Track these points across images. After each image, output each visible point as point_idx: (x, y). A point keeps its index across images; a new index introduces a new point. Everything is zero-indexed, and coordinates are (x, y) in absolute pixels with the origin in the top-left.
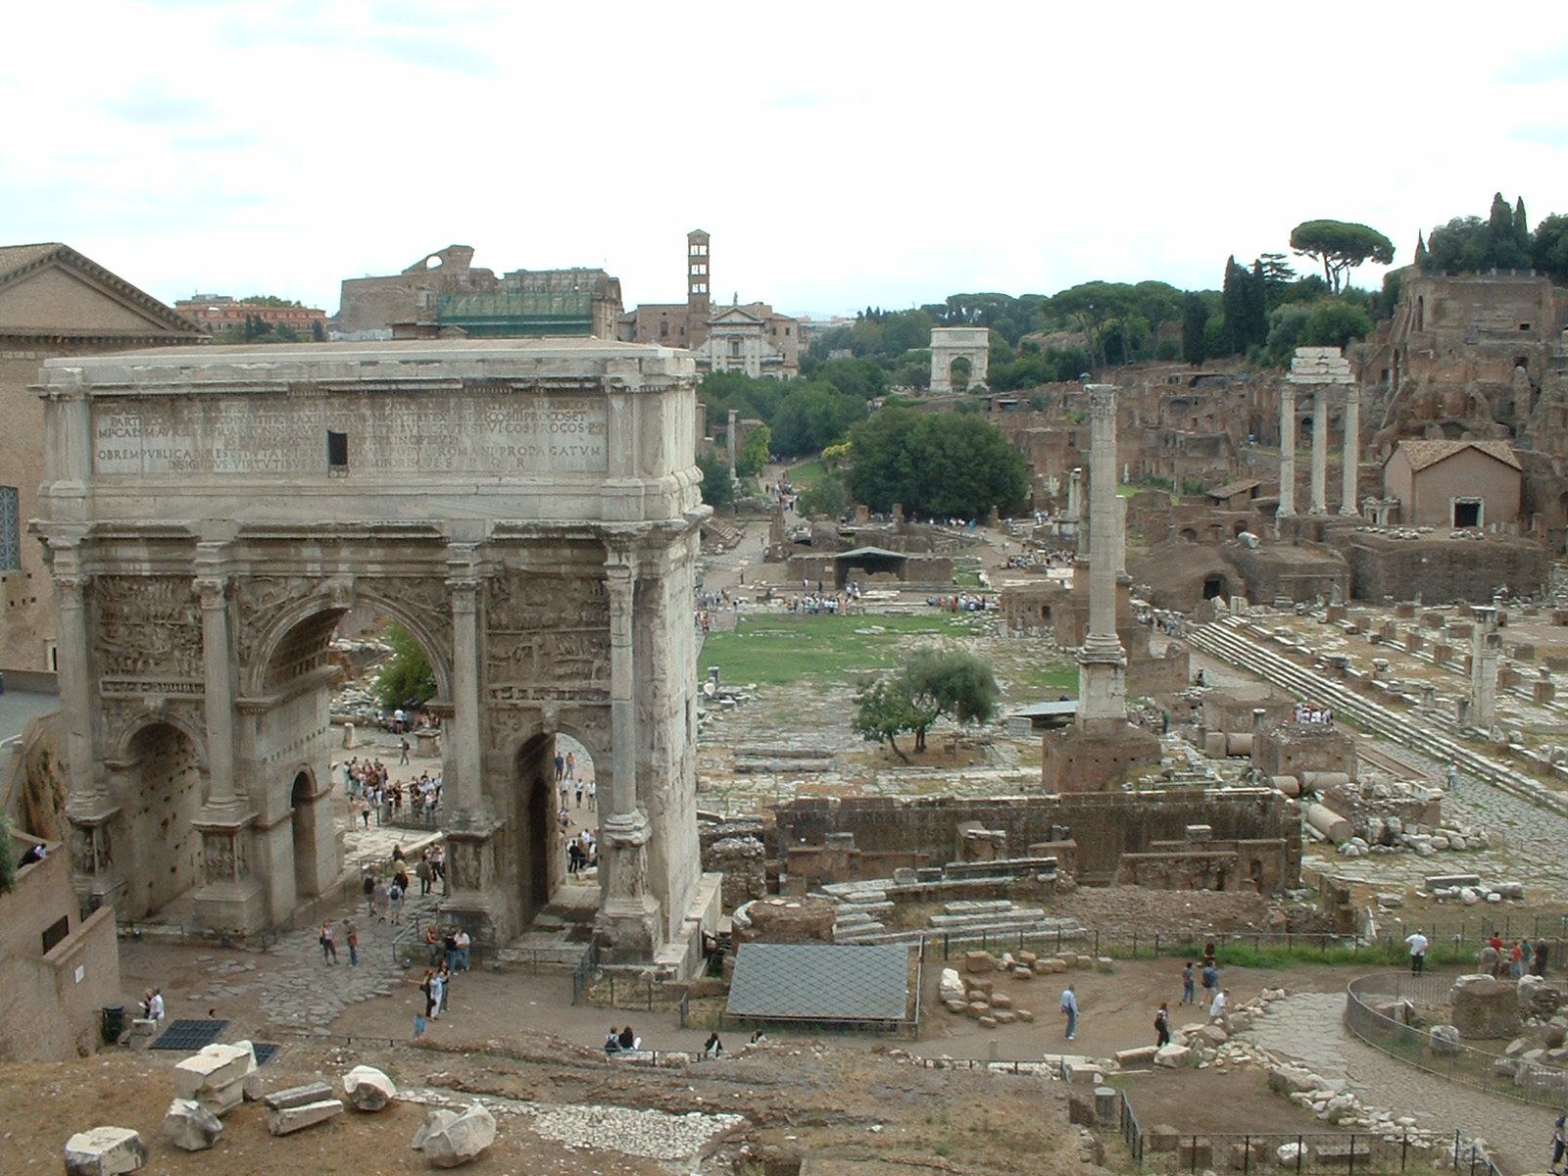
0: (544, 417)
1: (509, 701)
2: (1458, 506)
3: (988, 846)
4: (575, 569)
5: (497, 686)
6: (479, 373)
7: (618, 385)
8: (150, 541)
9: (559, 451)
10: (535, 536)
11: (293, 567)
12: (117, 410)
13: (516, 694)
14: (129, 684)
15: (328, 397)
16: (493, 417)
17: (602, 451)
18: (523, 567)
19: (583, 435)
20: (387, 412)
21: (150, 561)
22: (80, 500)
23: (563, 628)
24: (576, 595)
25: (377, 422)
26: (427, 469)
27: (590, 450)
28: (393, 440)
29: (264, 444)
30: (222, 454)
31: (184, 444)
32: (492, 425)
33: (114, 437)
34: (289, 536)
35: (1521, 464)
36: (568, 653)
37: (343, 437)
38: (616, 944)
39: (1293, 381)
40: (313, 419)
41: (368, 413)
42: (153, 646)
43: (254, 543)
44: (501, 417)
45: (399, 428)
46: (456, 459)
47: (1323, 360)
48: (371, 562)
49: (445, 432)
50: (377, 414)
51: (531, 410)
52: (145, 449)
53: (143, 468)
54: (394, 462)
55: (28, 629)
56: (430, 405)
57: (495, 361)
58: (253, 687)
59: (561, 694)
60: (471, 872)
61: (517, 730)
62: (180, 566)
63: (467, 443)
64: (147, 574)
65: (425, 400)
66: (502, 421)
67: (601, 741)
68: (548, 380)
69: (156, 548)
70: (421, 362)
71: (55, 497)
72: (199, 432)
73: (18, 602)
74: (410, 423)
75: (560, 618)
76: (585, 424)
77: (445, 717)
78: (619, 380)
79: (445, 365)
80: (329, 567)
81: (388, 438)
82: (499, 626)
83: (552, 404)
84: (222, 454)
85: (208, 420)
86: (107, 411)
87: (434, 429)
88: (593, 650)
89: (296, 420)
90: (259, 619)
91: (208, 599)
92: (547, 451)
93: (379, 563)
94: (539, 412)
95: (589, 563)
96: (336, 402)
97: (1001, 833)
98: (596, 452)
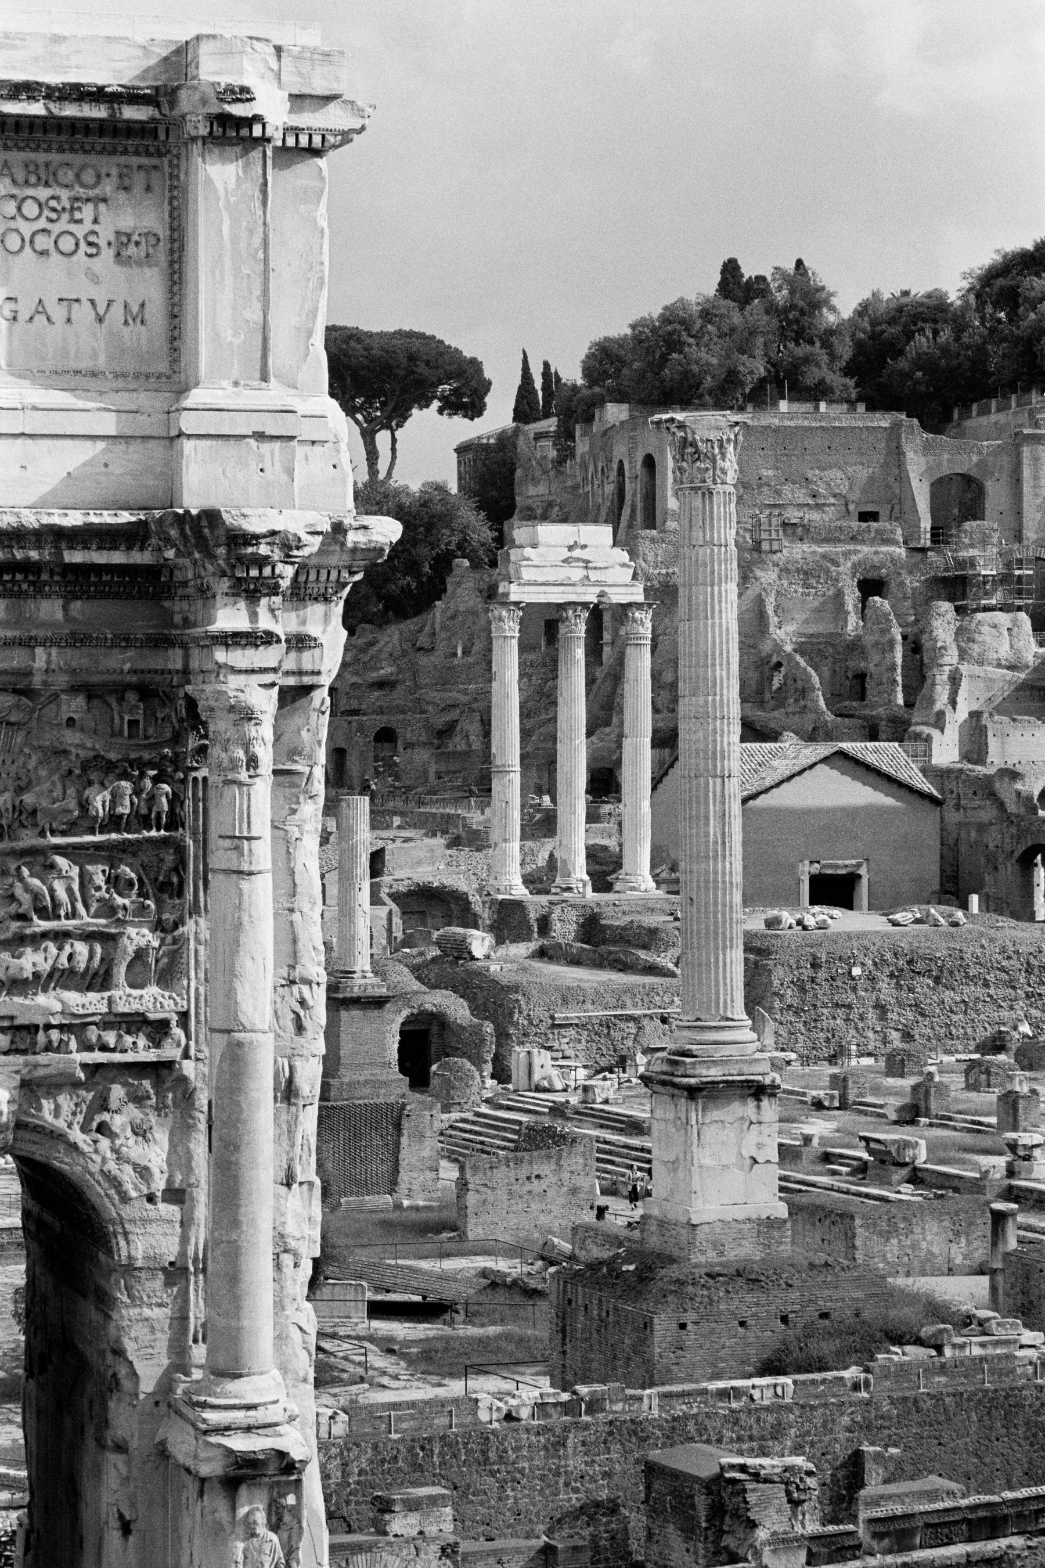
2: (816, 881)
3: (778, 1492)
4: (78, 658)
7: (238, 110)
17: (156, 312)
19: (96, 264)
23: (28, 839)
24: (71, 738)
27: (117, 311)
35: (941, 791)
36: (43, 913)
39: (513, 598)
47: (577, 553)
75: (18, 809)
76: (105, 234)
78: (243, 95)
95: (123, 641)
97: (799, 1461)
98: (136, 316)
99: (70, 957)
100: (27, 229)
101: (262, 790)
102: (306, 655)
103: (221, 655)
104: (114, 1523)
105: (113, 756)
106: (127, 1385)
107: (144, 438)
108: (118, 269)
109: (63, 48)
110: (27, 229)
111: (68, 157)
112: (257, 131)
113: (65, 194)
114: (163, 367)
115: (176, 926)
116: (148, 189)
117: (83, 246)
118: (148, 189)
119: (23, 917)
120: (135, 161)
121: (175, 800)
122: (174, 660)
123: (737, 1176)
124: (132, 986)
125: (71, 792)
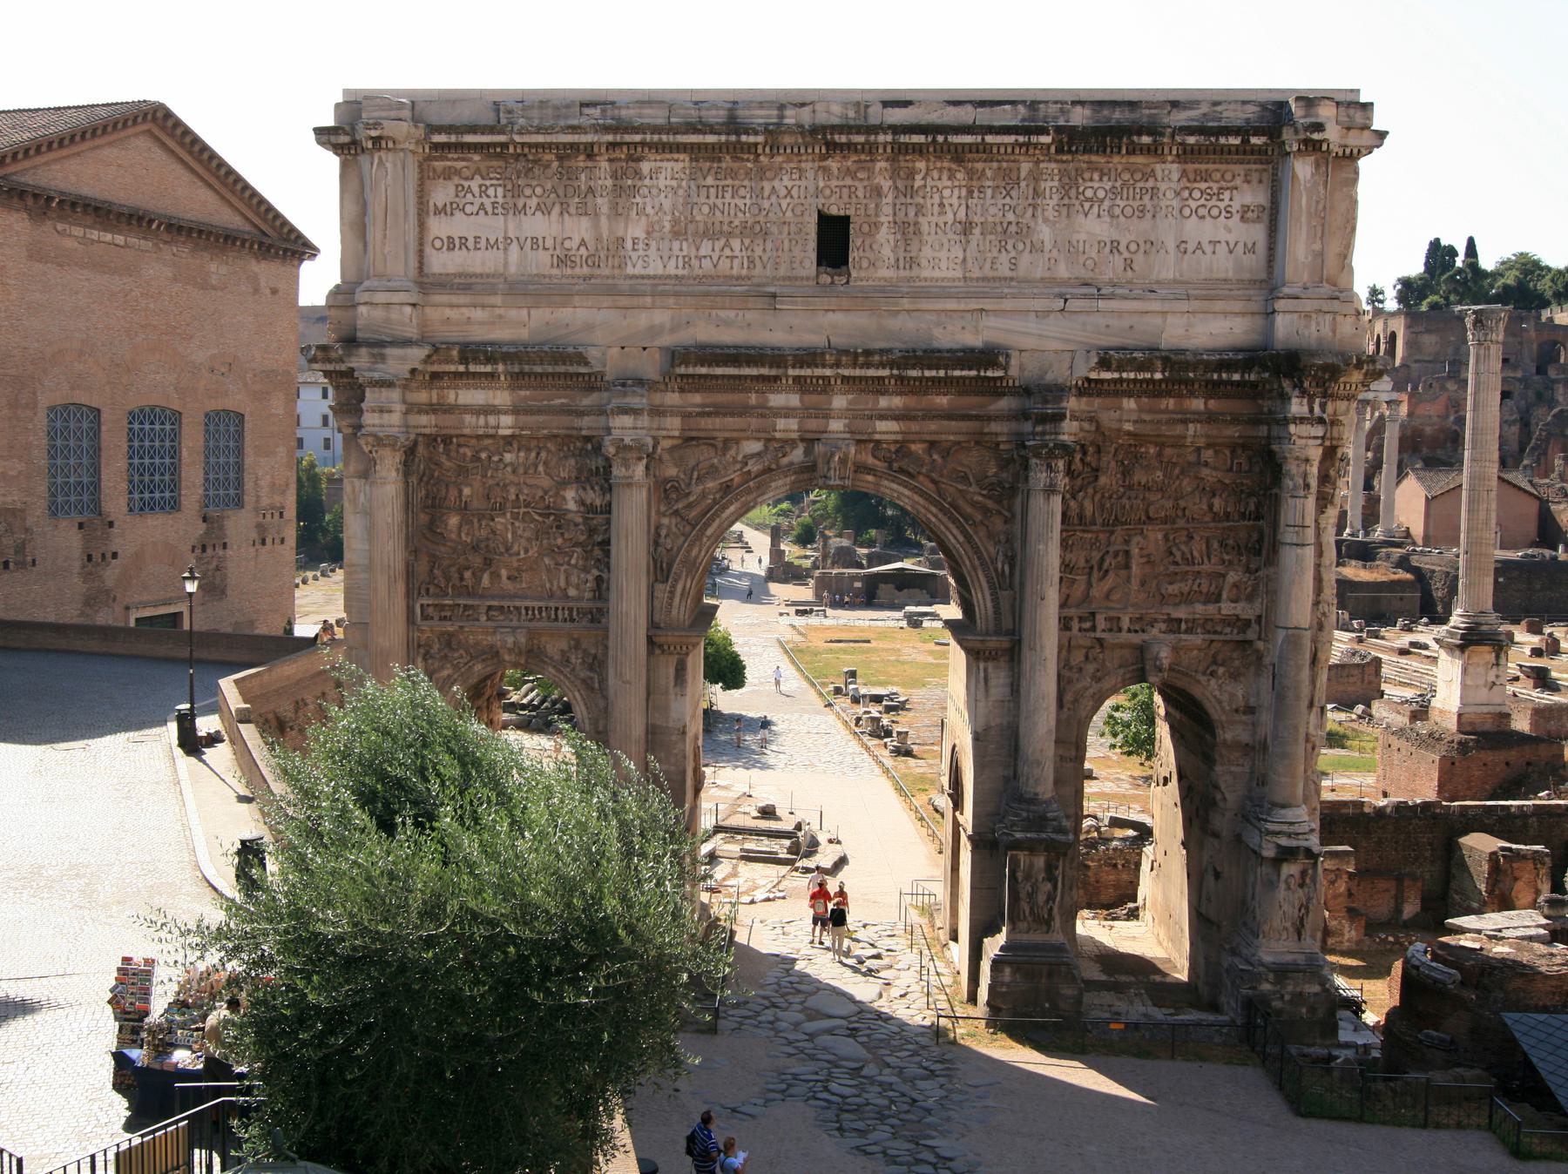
0: (1170, 194)
1: (1093, 635)
5: (1072, 612)
6: (1079, 117)
7: (1316, 136)
8: (518, 380)
9: (1191, 247)
10: (1158, 376)
11: (754, 422)
12: (466, 173)
13: (1101, 623)
14: (465, 606)
15: (823, 158)
16: (1089, 193)
18: (1128, 427)
19: (1230, 222)
20: (918, 183)
21: (516, 411)
22: (408, 309)
24: (1205, 472)
25: (902, 200)
26: (976, 273)
27: (1240, 247)
28: (925, 228)
29: (710, 233)
30: (641, 246)
31: (578, 229)
32: (1087, 205)
33: (458, 215)
34: (754, 371)
37: (845, 221)
38: (1279, 1012)
40: (795, 192)
41: (886, 184)
42: (507, 550)
43: (691, 384)
44: (1101, 194)
45: (936, 208)
46: (1025, 259)
48: (882, 417)
49: (1010, 217)
50: (900, 184)
51: (1150, 183)
52: (511, 234)
53: (506, 265)
54: (924, 263)
55: (107, 592)
56: (989, 173)
57: (1101, 104)
58: (674, 612)
59: (1174, 625)
60: (1041, 898)
61: (1099, 680)
62: (565, 420)
63: (1044, 233)
64: (508, 432)
65: (979, 166)
66: (1102, 201)
67: (1232, 696)
68: (1190, 130)
69: (523, 393)
70: (982, 104)
71: (366, 303)
72: (605, 209)
73: (97, 557)
74: (955, 201)
76: (1236, 206)
77: (986, 660)
78: (1319, 127)
79: (1021, 108)
80: (812, 424)
81: (916, 223)
82: (1081, 517)
83: (1184, 173)
84: (641, 246)
85: (618, 190)
86: (448, 174)
87: (993, 210)
88: (1227, 557)
89: (766, 194)
90: (690, 506)
91: (627, 467)
92: (1171, 245)
93: (896, 418)
94: (1163, 186)
95: (1235, 420)
96: (833, 164)
99: (1200, 585)
100: (1193, 205)
101: (1311, 503)
102: (1335, 428)
103: (1292, 428)
104: (1211, 872)
105: (1227, 481)
106: (1221, 804)
107: (1253, 314)
108: (1241, 224)
109: (1219, 108)
110: (1193, 205)
111: (1217, 166)
112: (1324, 147)
113: (1215, 186)
114: (1263, 276)
115: (1257, 571)
116: (1260, 181)
117: (1224, 213)
118: (1260, 181)
119: (1176, 563)
120: (1254, 167)
121: (1259, 505)
122: (1263, 430)
123: (1485, 691)
124: (1232, 601)
125: (1204, 500)
